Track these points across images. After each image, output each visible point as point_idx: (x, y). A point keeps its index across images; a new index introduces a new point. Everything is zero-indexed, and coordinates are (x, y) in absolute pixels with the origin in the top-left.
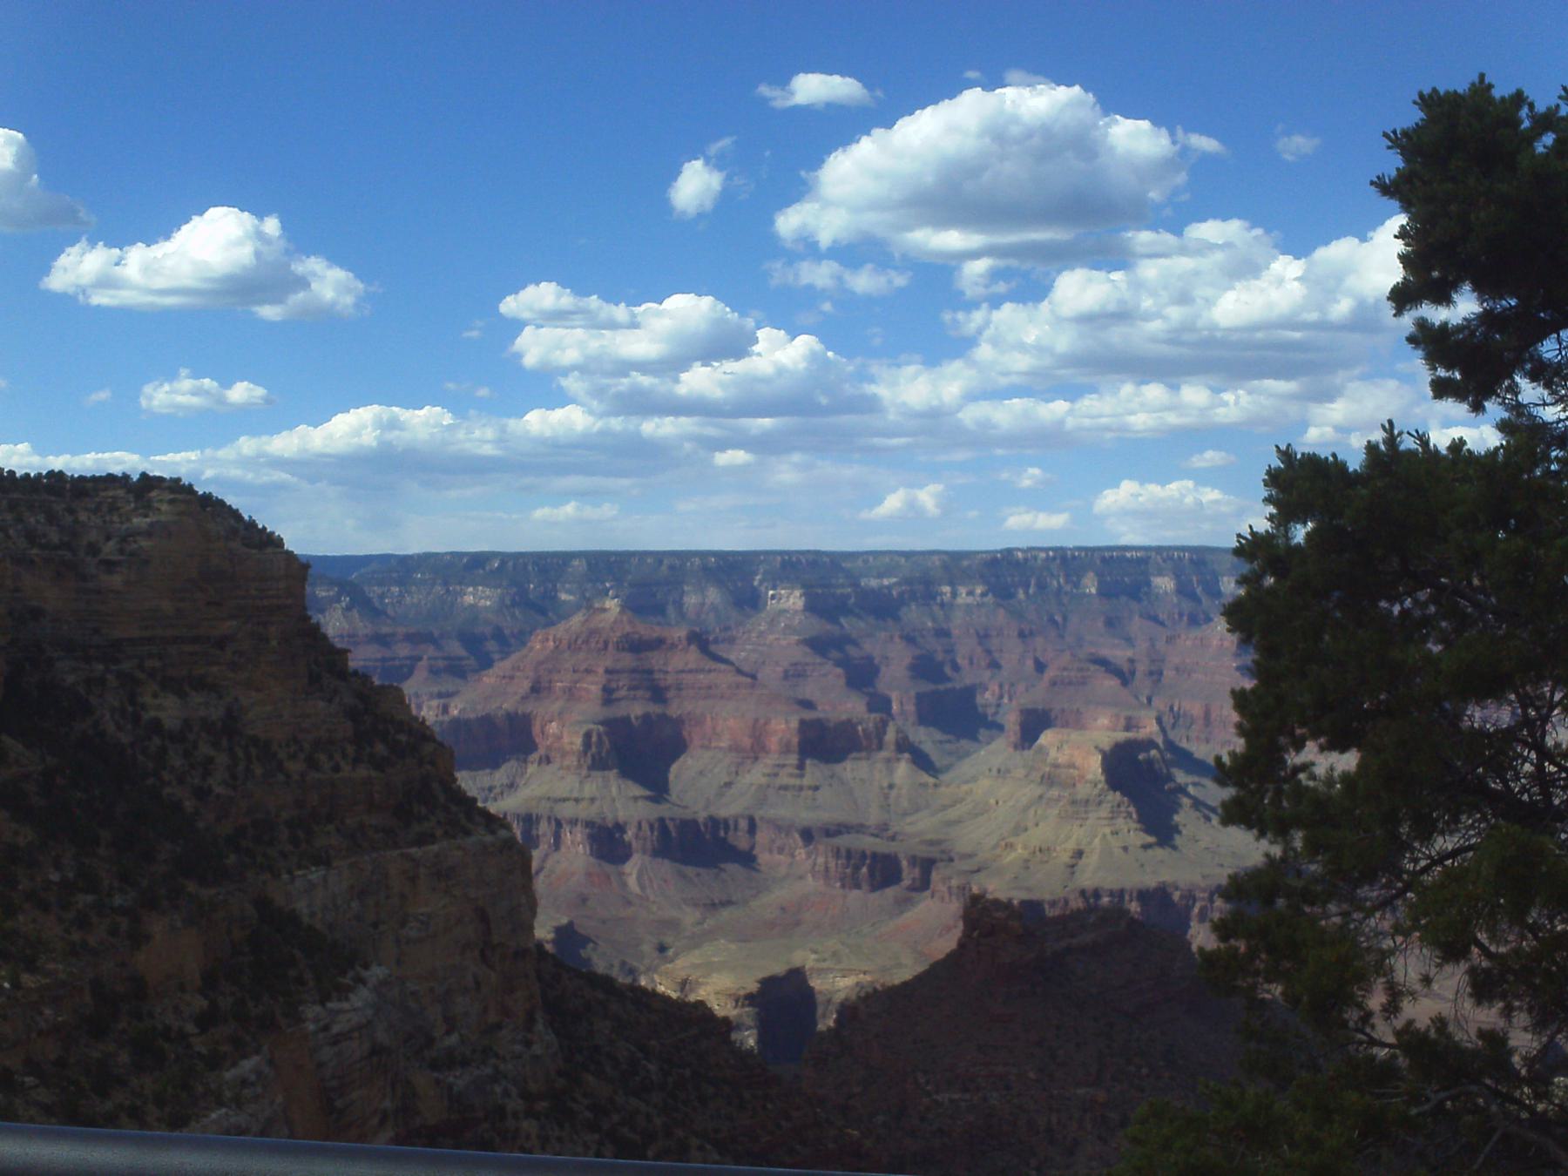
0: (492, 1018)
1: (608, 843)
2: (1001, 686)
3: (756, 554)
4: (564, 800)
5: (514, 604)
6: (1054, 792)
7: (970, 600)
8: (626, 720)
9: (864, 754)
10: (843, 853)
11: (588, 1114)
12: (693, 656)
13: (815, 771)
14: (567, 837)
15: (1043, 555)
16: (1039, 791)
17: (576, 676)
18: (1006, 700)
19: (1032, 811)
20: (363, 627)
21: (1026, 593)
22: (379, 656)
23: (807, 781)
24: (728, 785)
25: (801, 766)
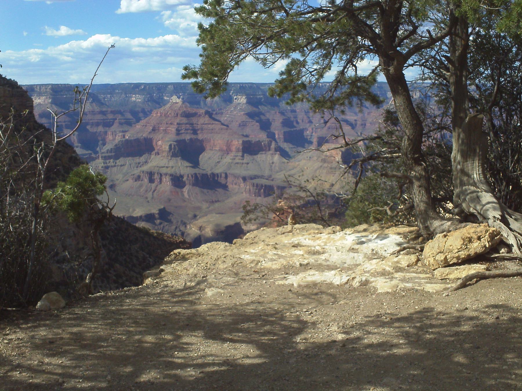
0: (81, 246)
1: (178, 181)
2: (312, 129)
5: (148, 101)
6: (326, 165)
8: (184, 141)
9: (264, 152)
10: (255, 185)
11: (114, 278)
12: (207, 119)
13: (247, 158)
14: (164, 179)
15: (328, 84)
16: (320, 164)
17: (167, 126)
18: (314, 134)
19: (318, 171)
20: (97, 109)
22: (102, 118)
23: (245, 161)
24: (219, 162)
25: (243, 156)
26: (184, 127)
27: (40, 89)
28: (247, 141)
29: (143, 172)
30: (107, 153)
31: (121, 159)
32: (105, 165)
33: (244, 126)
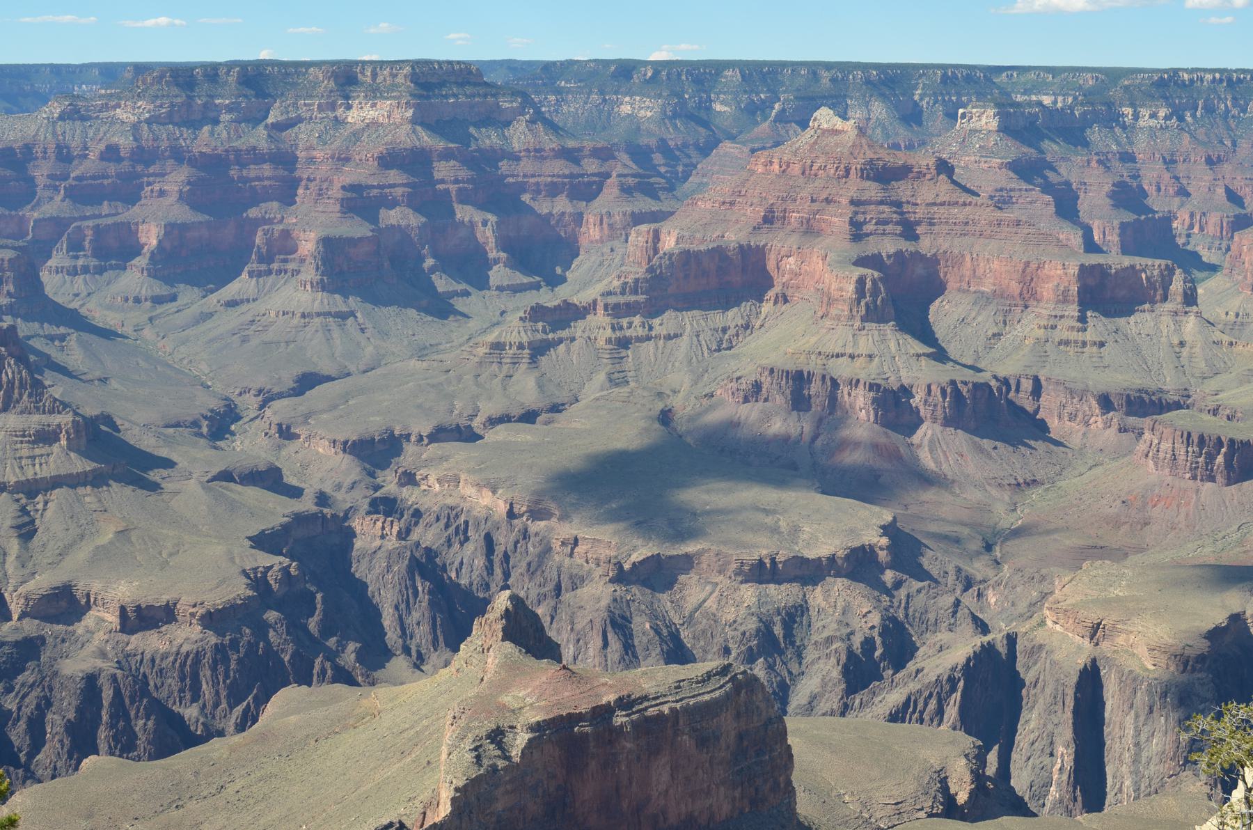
2: (1192, 215)
3: (915, 67)
4: (837, 356)
5: (675, 115)
7: (1153, 122)
9: (1147, 306)
10: (1195, 438)
13: (1098, 325)
15: (1209, 77)
17: (816, 206)
18: (1196, 230)
20: (550, 142)
21: (1194, 116)
22: (567, 172)
23: (1089, 336)
24: (997, 335)
25: (1082, 319)
26: (872, 212)
27: (374, 75)
28: (1093, 267)
29: (772, 371)
30: (623, 293)
31: (669, 314)
32: (618, 334)
33: (1004, 202)
